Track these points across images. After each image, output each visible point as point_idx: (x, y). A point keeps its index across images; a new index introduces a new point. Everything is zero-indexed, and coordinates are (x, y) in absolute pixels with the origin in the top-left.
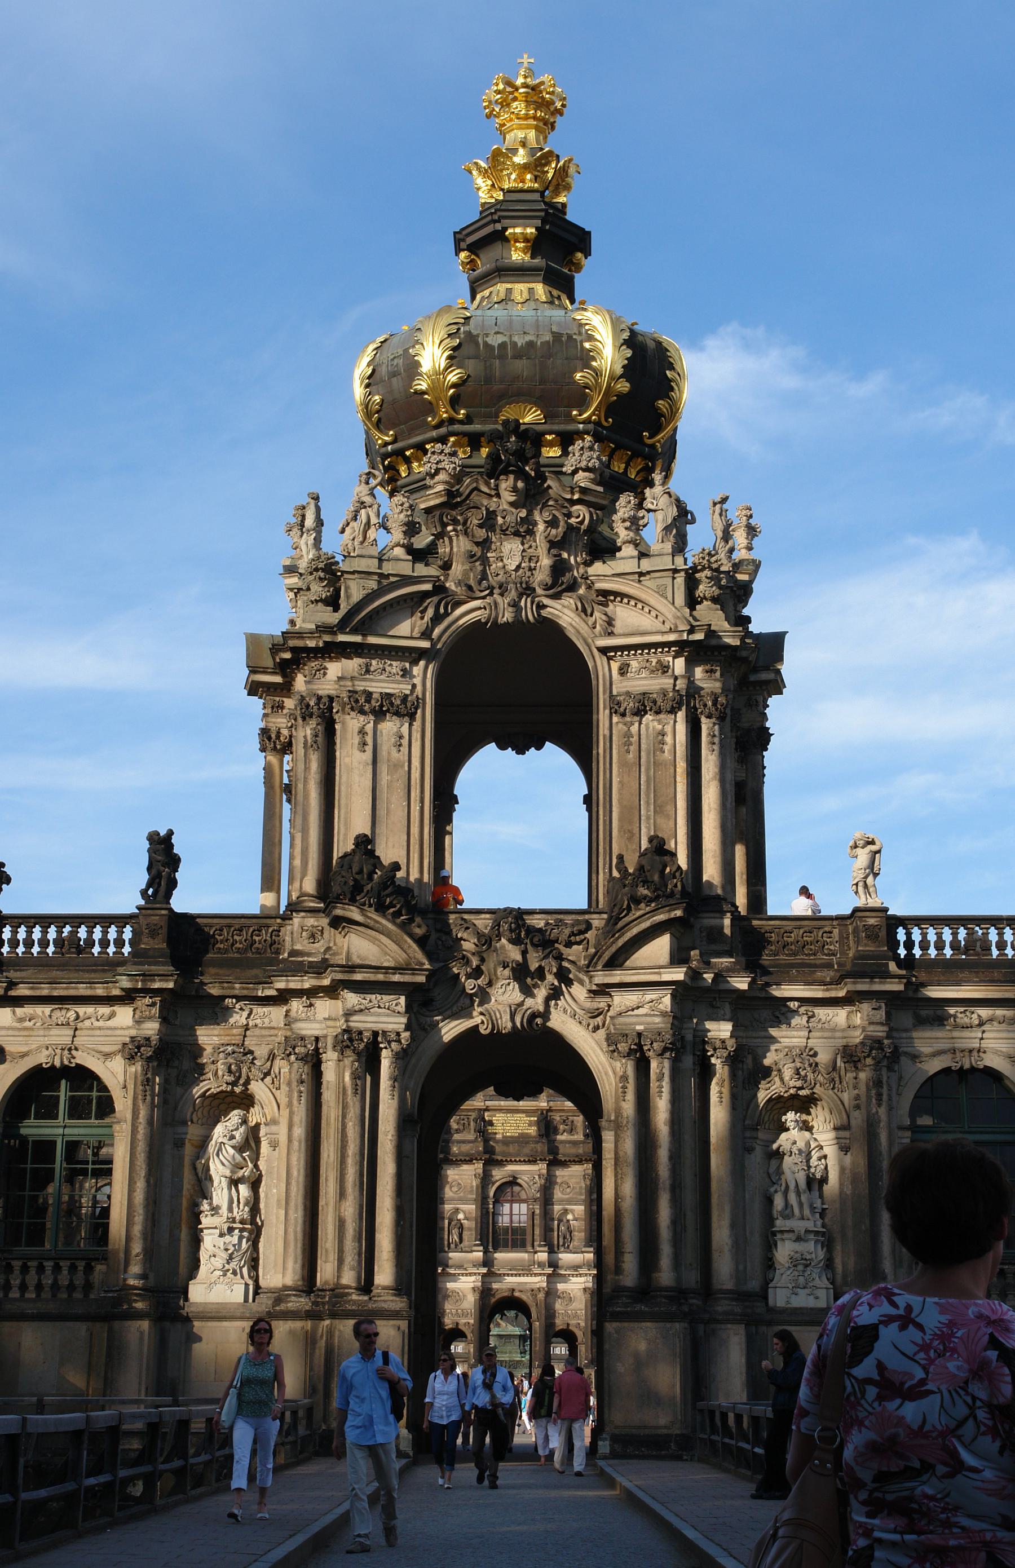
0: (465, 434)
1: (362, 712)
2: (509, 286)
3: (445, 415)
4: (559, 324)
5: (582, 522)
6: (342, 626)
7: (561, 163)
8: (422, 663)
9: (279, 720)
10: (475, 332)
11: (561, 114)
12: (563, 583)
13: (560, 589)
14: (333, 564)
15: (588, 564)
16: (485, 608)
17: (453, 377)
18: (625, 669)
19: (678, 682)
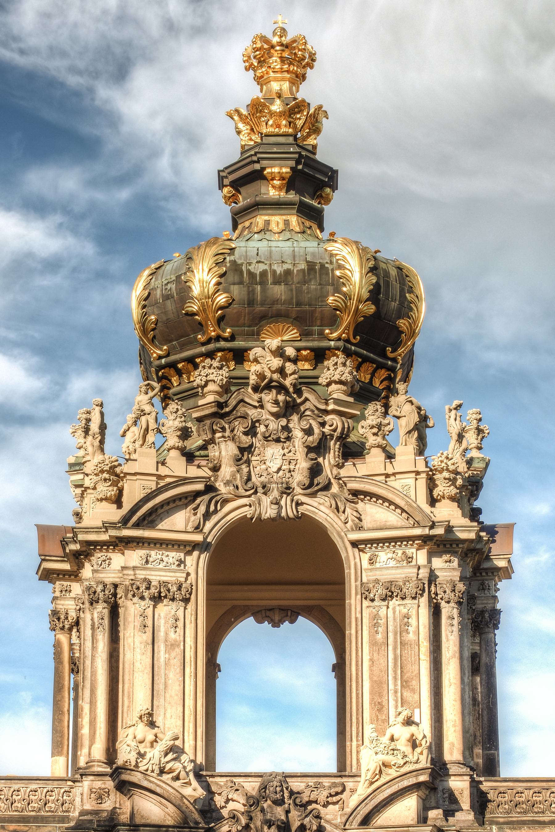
0: (230, 350)
1: (142, 598)
2: (266, 218)
3: (213, 334)
4: (313, 254)
5: (335, 430)
6: (125, 521)
7: (312, 111)
8: (196, 553)
9: (67, 602)
10: (239, 262)
11: (312, 68)
12: (318, 485)
13: (316, 488)
14: (115, 467)
15: (340, 466)
16: (250, 506)
17: (222, 299)
18: (374, 560)
19: (421, 571)
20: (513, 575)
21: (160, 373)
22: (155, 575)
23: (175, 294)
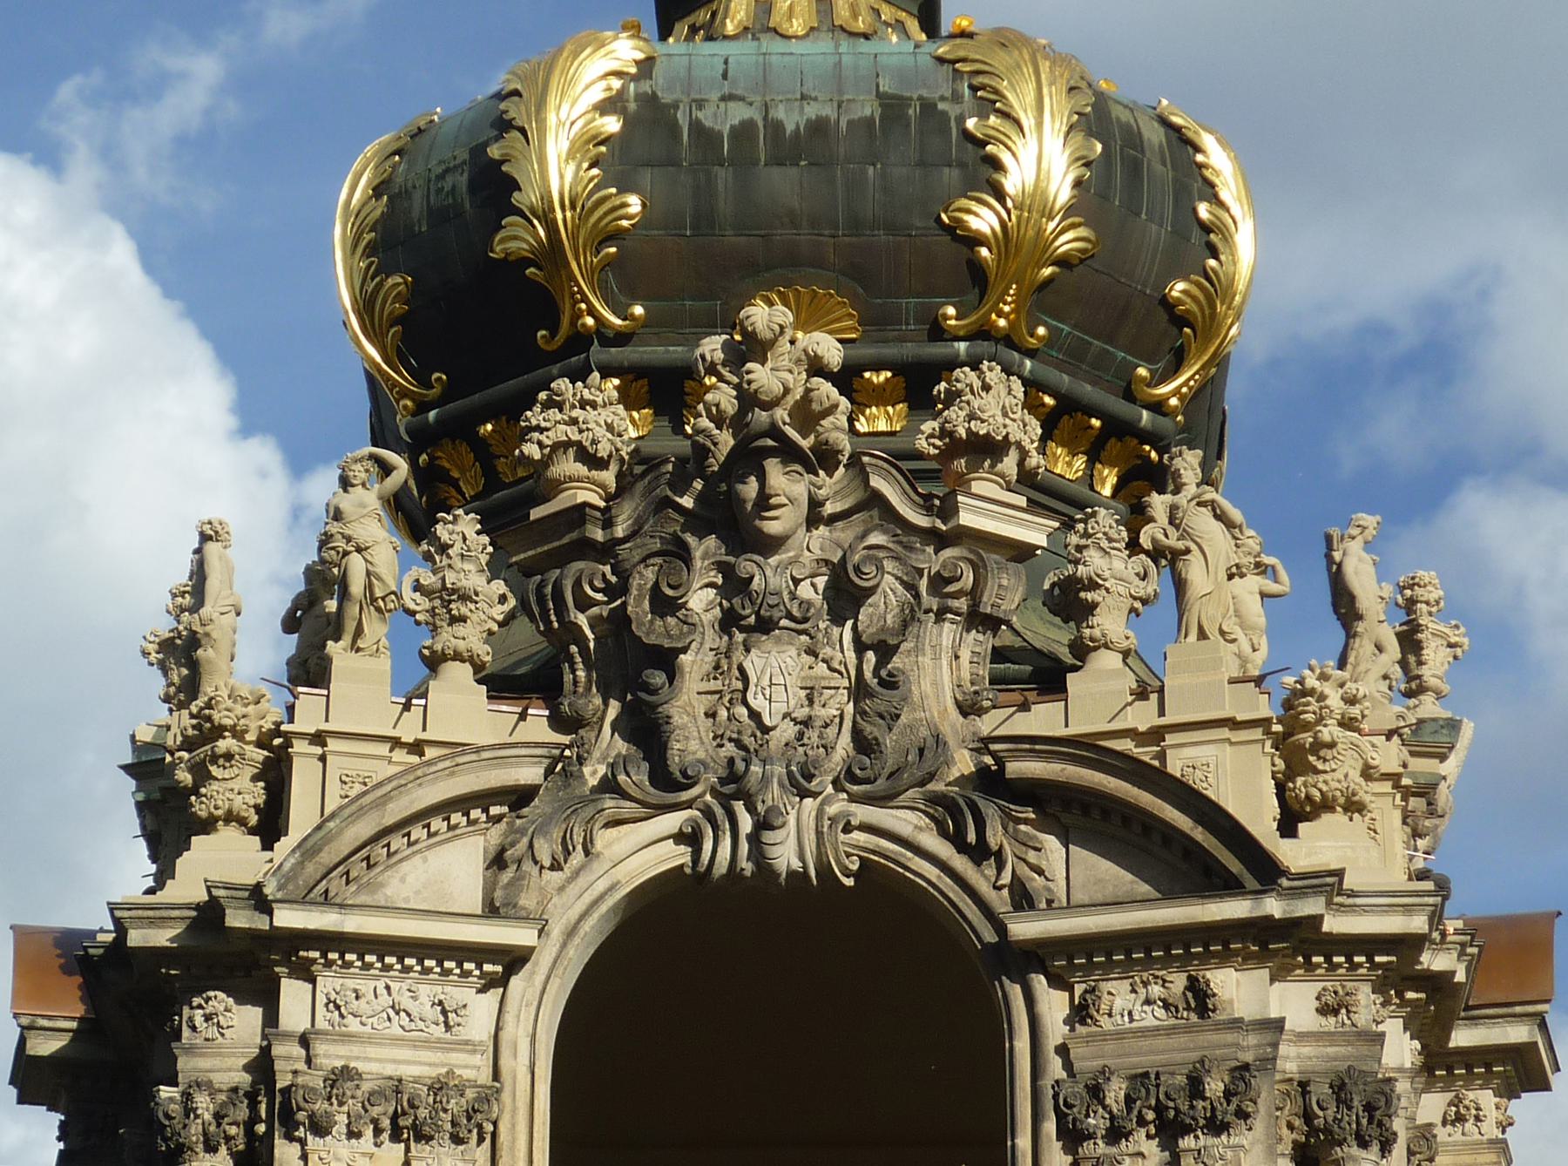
10: (666, 98)
20: (1554, 1079)
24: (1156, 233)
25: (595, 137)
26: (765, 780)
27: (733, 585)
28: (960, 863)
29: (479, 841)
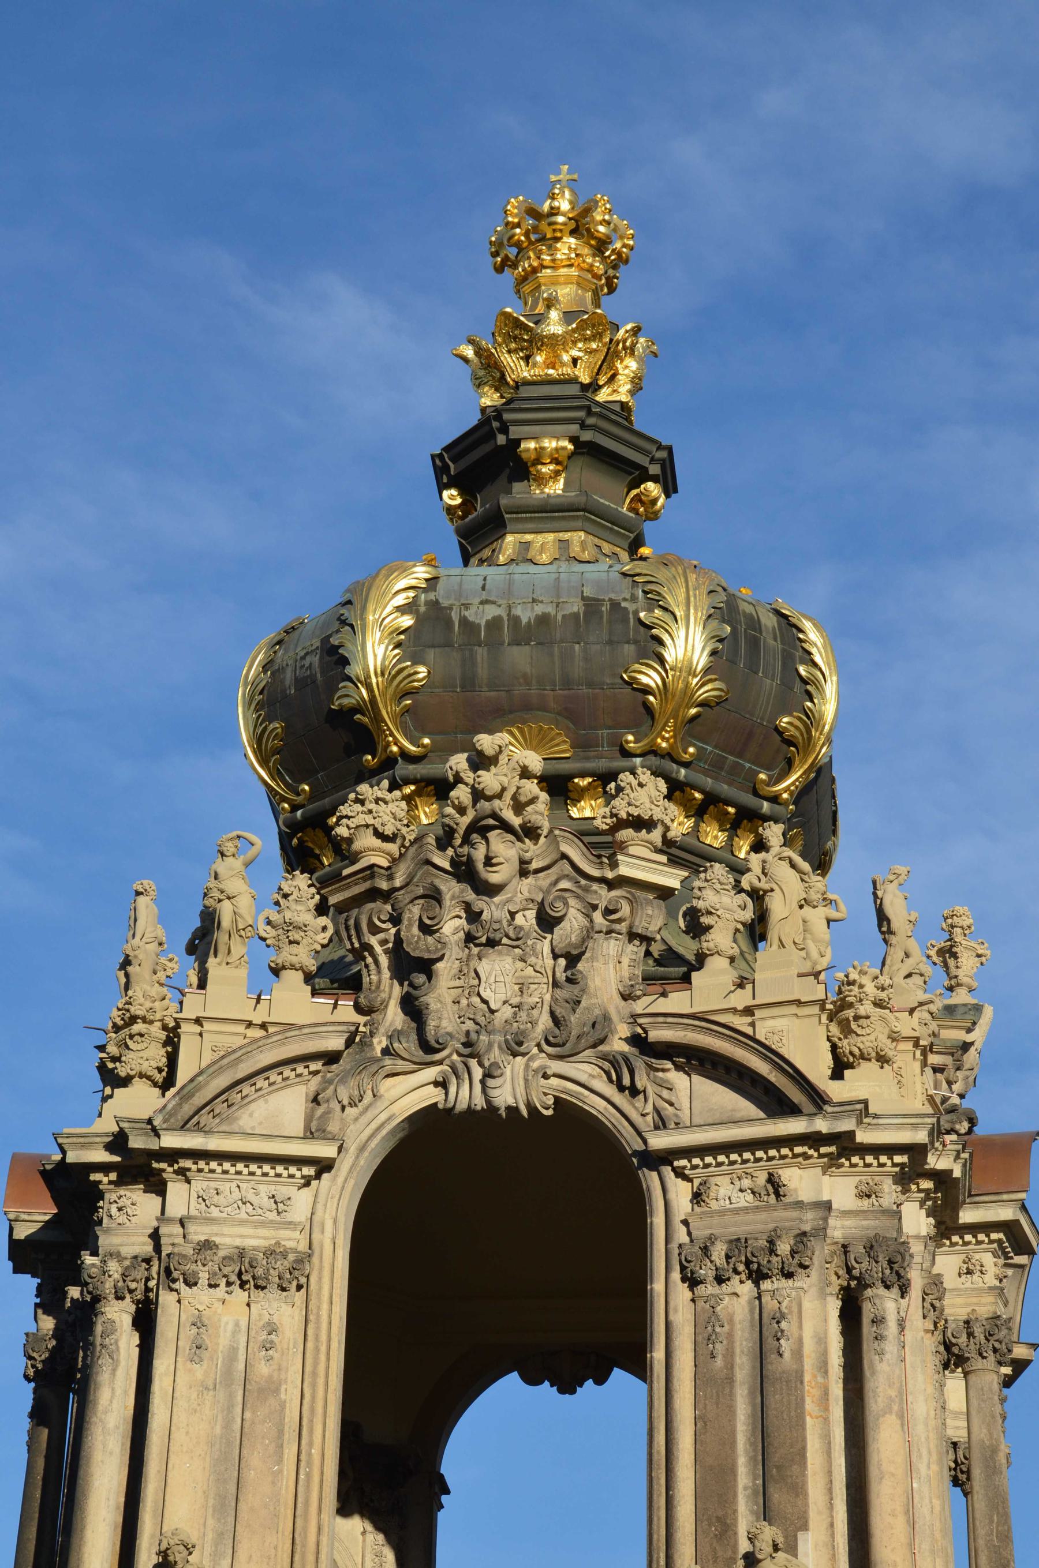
10: (445, 603)
21: (295, 841)
22: (231, 1236)
23: (319, 675)
24: (769, 685)
25: (397, 629)
26: (490, 1045)
27: (473, 916)
28: (618, 1098)
29: (302, 1089)
